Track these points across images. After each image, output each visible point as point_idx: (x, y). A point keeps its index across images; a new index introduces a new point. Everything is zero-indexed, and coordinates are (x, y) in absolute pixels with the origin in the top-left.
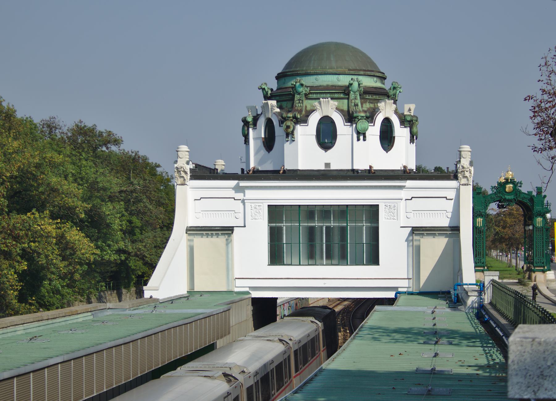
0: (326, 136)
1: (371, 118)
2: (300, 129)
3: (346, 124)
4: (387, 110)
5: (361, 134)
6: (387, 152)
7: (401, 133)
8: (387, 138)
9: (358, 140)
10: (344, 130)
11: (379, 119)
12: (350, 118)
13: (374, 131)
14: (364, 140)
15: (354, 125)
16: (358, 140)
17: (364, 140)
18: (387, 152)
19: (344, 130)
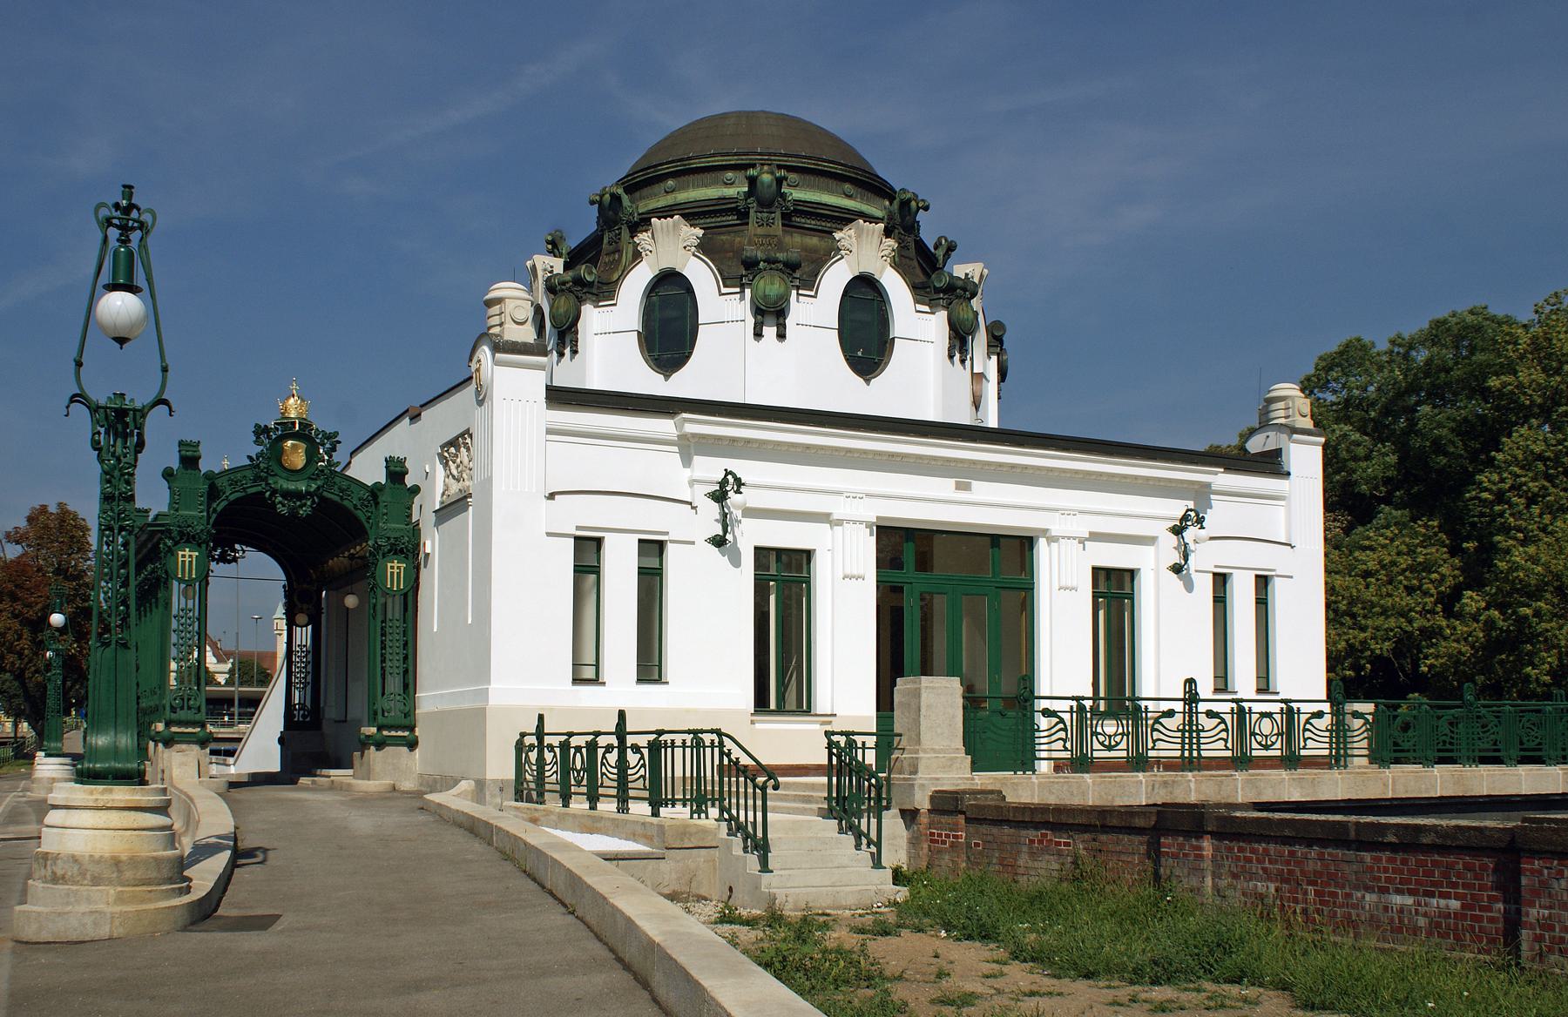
0: (669, 331)
1: (804, 274)
2: (593, 318)
3: (724, 290)
4: (864, 251)
5: (771, 314)
6: (868, 381)
7: (917, 328)
8: (865, 338)
9: (758, 335)
10: (721, 310)
11: (835, 278)
12: (737, 271)
13: (817, 311)
14: (781, 336)
15: (748, 291)
16: (758, 335)
17: (781, 336)
18: (868, 381)
19: (721, 310)
